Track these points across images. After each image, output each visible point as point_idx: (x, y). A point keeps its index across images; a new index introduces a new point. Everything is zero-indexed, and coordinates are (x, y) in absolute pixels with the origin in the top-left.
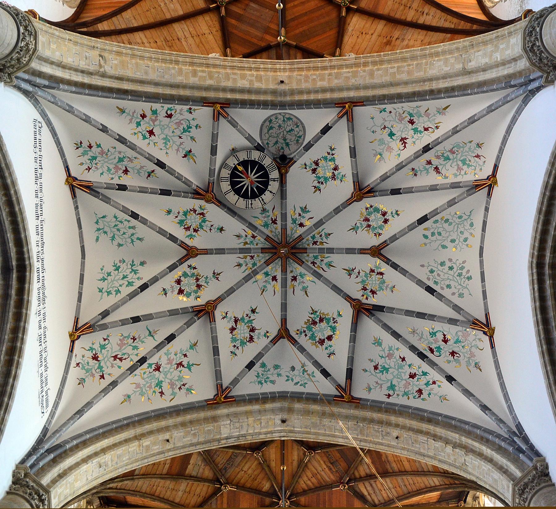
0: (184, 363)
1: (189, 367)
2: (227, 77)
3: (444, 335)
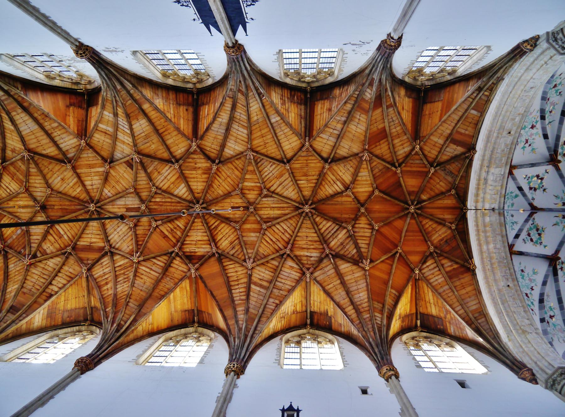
3: (553, 316)
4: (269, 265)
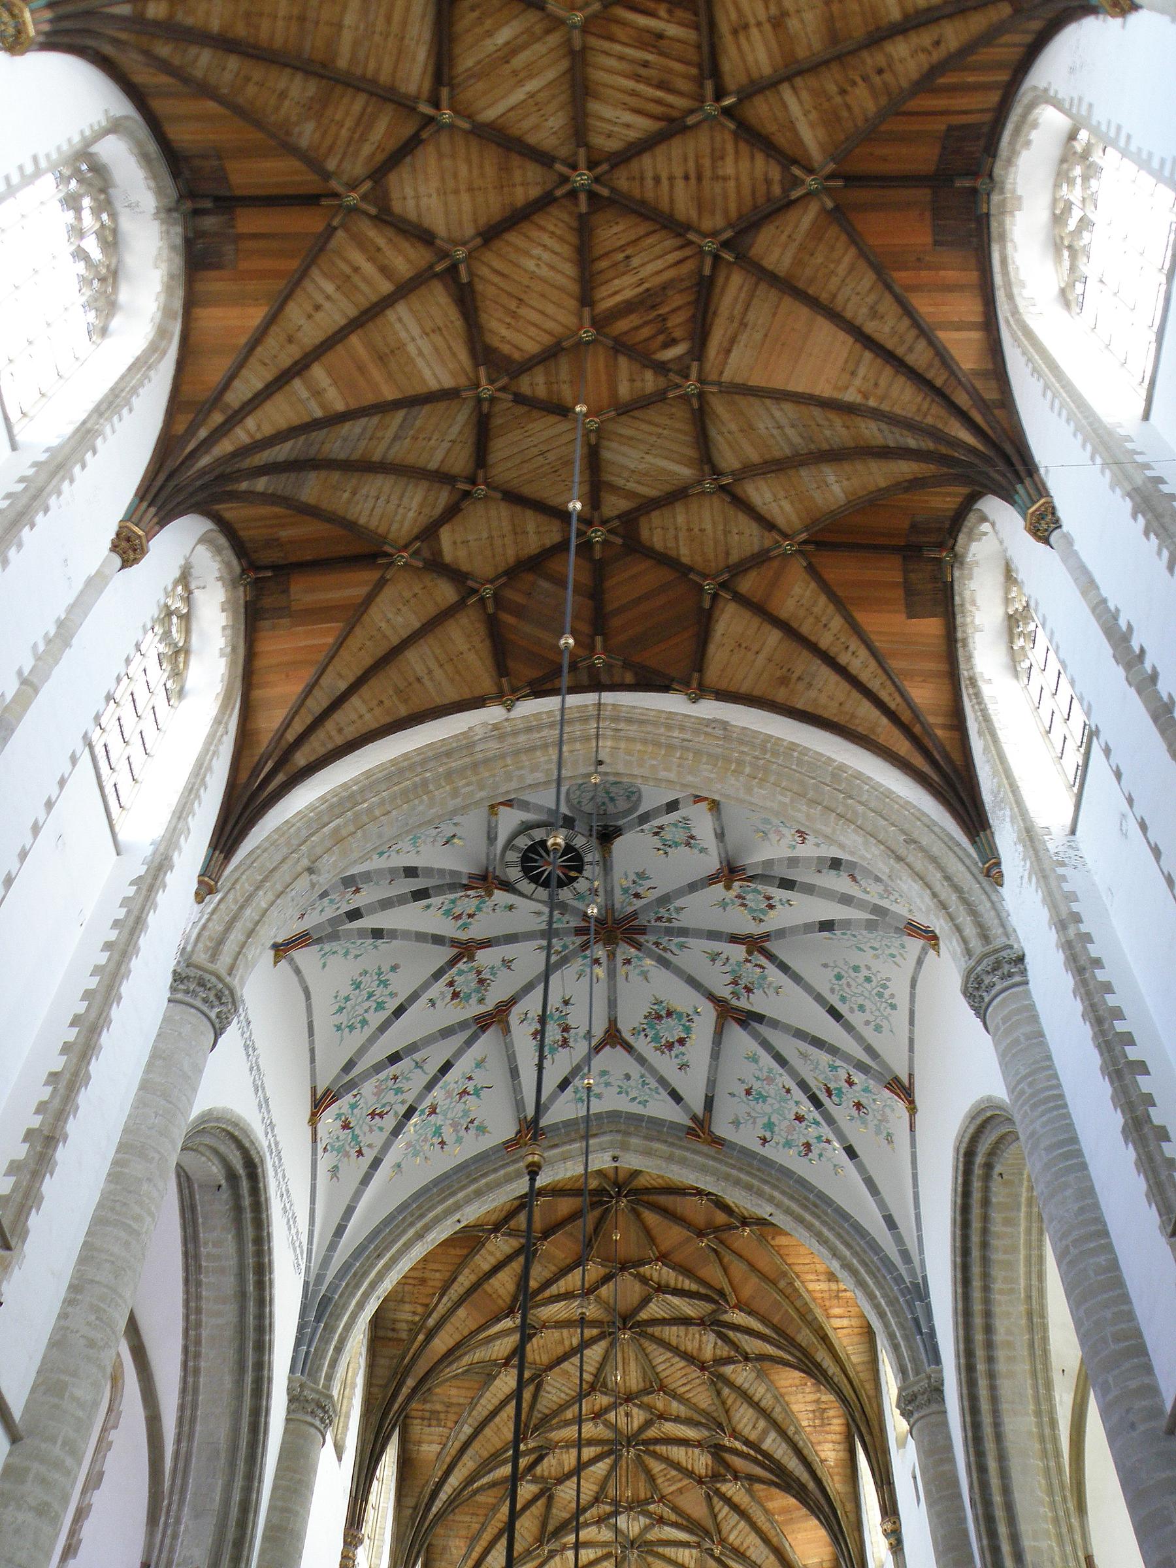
0: (471, 1090)
1: (477, 1092)
2: (509, 777)
4: (729, 1402)
